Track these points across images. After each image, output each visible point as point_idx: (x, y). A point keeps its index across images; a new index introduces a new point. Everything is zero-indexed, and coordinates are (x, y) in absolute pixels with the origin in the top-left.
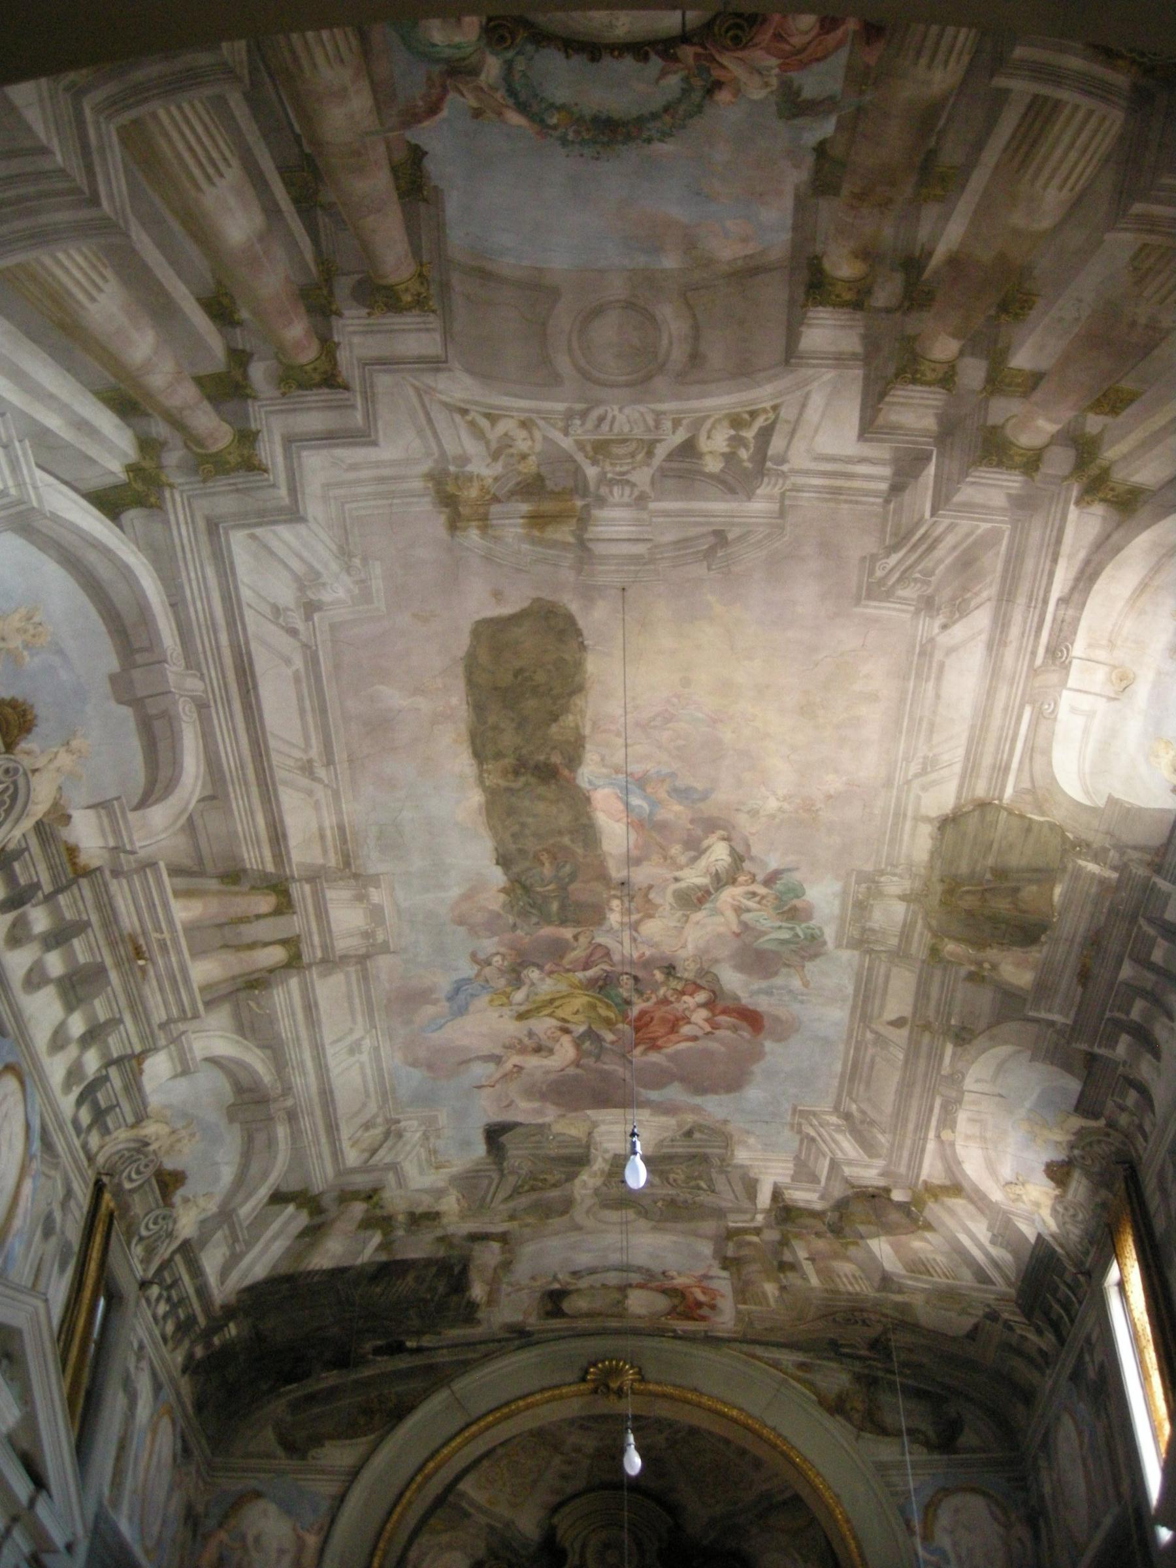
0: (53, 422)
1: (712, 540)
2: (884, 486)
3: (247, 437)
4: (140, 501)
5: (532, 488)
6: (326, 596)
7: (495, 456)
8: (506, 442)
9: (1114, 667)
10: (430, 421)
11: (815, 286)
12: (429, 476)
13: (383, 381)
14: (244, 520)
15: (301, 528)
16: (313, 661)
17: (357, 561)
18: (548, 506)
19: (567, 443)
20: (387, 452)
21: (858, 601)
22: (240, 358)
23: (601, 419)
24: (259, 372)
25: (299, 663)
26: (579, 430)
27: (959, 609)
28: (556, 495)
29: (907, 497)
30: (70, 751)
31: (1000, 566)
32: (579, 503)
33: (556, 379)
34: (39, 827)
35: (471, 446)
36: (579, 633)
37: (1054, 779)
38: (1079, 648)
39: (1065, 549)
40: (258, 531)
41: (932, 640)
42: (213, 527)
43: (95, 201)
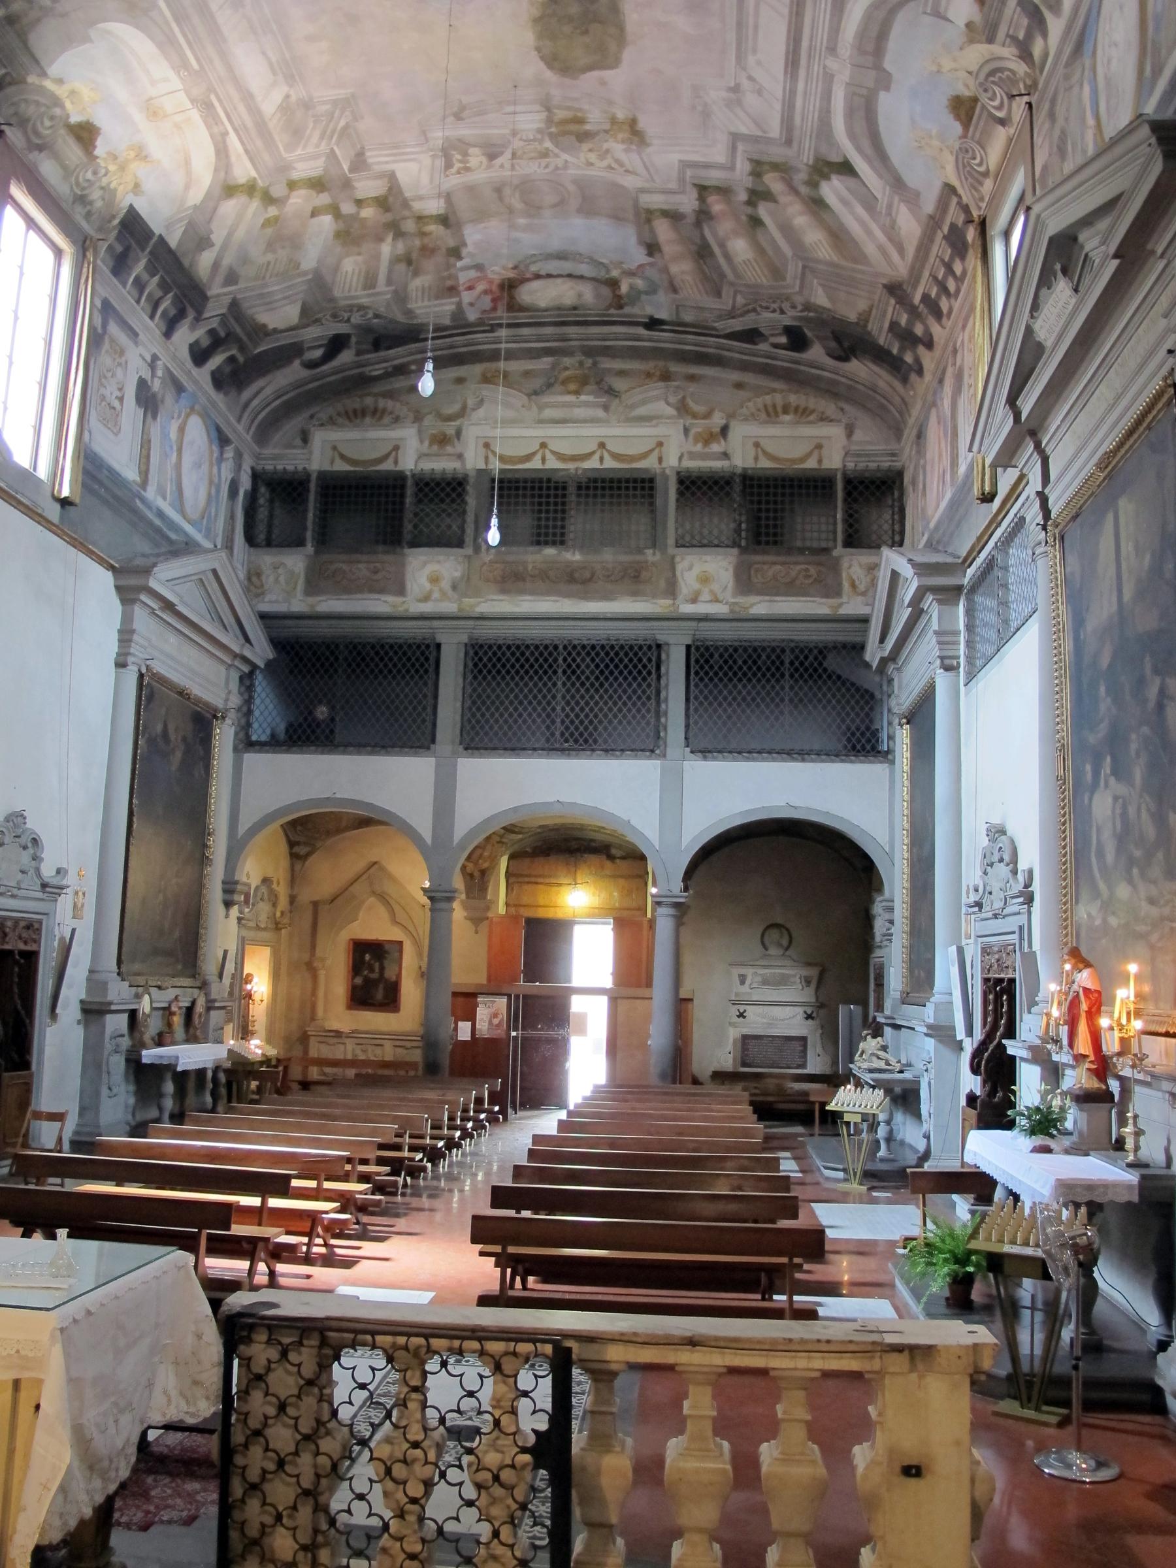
0: (860, 210)
1: (464, 115)
2: (368, 154)
3: (756, 174)
4: (829, 164)
5: (583, 137)
6: (724, 94)
7: (607, 151)
8: (602, 157)
9: (165, 116)
10: (647, 169)
11: (444, 220)
12: (648, 145)
13: (673, 185)
14: (769, 141)
15: (733, 129)
16: (740, 58)
17: (700, 108)
18: (574, 127)
19: (565, 156)
20: (674, 157)
21: (353, 96)
22: (751, 203)
23: (547, 167)
24: (743, 196)
25: (751, 60)
26: (559, 162)
27: (285, 108)
28: (570, 133)
29: (353, 153)
30: (939, 65)
31: (277, 138)
32: (553, 130)
33: (576, 182)
34: (990, 40)
35: (623, 157)
36: (542, 58)
37: (137, 27)
38: (195, 115)
39: (245, 158)
40: (760, 133)
41: (291, 86)
42: (789, 142)
43: (804, 267)
